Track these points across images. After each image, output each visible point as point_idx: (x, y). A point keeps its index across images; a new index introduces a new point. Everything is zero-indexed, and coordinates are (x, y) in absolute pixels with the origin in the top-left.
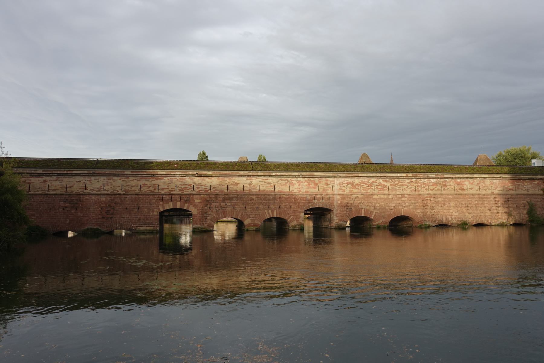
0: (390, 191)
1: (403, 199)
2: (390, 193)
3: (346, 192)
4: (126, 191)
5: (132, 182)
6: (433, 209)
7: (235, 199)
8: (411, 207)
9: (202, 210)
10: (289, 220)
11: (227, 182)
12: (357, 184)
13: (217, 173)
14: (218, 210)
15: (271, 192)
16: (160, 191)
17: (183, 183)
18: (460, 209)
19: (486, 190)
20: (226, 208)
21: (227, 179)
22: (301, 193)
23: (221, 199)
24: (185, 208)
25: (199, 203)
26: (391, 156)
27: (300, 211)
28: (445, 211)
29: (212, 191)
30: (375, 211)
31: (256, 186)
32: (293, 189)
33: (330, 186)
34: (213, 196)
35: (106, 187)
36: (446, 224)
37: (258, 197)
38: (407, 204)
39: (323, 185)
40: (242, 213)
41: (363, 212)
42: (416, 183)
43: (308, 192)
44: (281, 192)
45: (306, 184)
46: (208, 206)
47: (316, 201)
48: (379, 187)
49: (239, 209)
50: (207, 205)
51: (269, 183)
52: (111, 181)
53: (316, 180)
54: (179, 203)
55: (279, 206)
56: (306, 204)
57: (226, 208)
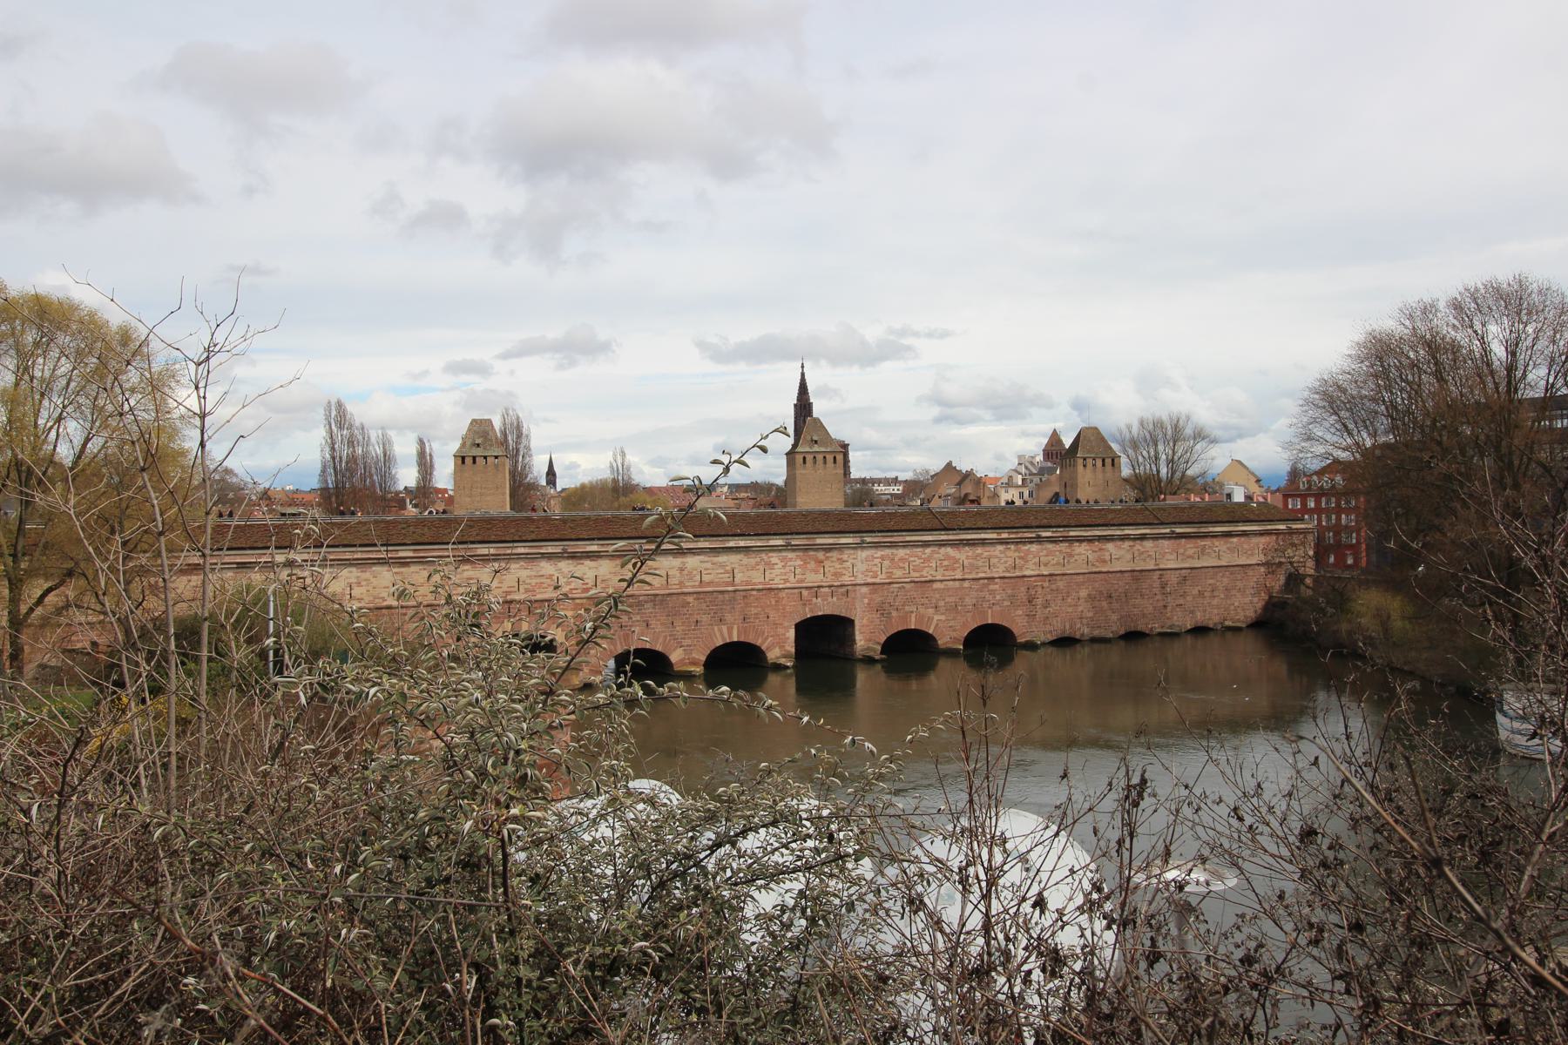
0: (966, 570)
1: (991, 587)
2: (966, 577)
3: (880, 577)
6: (1046, 605)
8: (1007, 603)
10: (763, 648)
12: (902, 559)
15: (727, 584)
17: (534, 573)
18: (1097, 603)
19: (1144, 560)
20: (631, 626)
22: (788, 585)
26: (803, 367)
27: (786, 624)
28: (1070, 610)
30: (936, 618)
31: (695, 572)
32: (772, 576)
36: (1072, 636)
38: (998, 597)
40: (666, 637)
41: (913, 619)
42: (1015, 551)
43: (802, 581)
44: (748, 583)
47: (819, 599)
48: (946, 563)
51: (722, 566)
52: (367, 575)
53: (820, 555)
55: (742, 617)
57: (631, 626)
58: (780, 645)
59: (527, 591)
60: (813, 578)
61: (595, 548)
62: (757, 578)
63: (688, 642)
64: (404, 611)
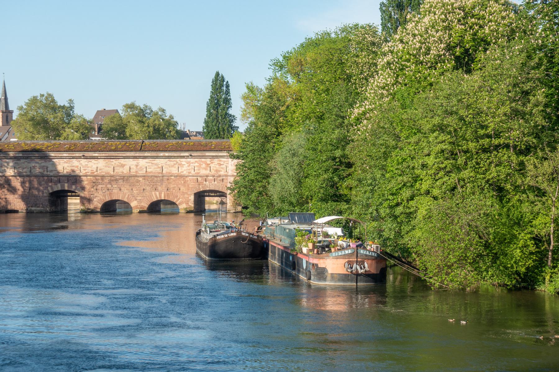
5: (23, 164)
11: (113, 163)
14: (104, 191)
15: (159, 173)
16: (48, 173)
17: (70, 165)
21: (113, 160)
22: (191, 174)
23: (106, 181)
27: (189, 193)
29: (98, 172)
31: (143, 167)
32: (183, 170)
37: (145, 179)
39: (215, 166)
40: (129, 195)
43: (198, 173)
44: (169, 173)
45: (196, 164)
46: (95, 188)
47: (207, 182)
49: (126, 191)
50: (94, 186)
51: (156, 164)
53: (208, 161)
60: (203, 172)
61: (96, 155)
62: (174, 171)
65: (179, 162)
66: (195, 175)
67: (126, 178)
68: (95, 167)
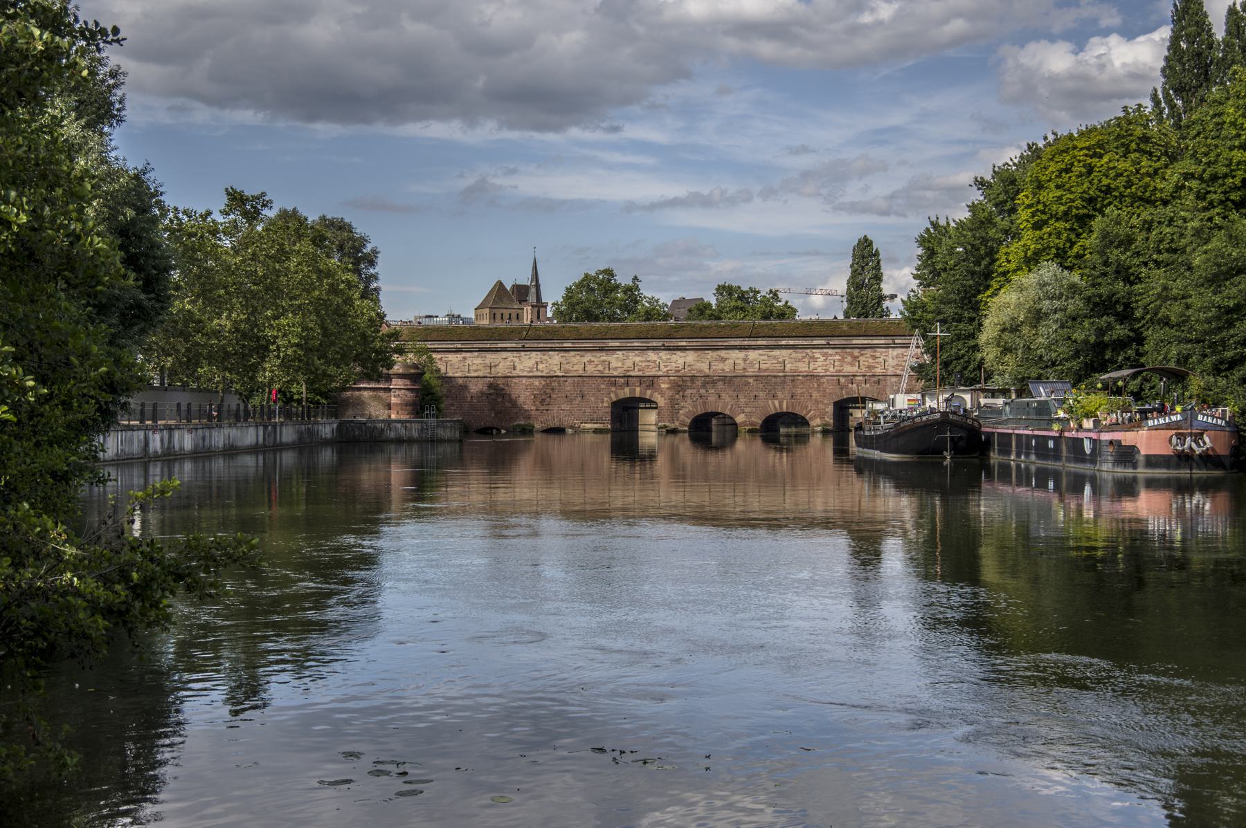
4: (567, 371)
5: (573, 359)
7: (721, 383)
9: (672, 399)
10: (807, 418)
13: (695, 343)
15: (779, 371)
21: (709, 352)
22: (828, 373)
23: (699, 383)
24: (647, 397)
25: (667, 389)
27: (826, 402)
33: (881, 360)
34: (688, 379)
35: (540, 367)
37: (757, 380)
40: (732, 405)
43: (840, 371)
44: (795, 371)
46: (681, 394)
47: (855, 385)
51: (775, 358)
52: (546, 357)
53: (856, 352)
54: (638, 389)
56: (838, 391)
58: (820, 416)
59: (639, 370)
60: (848, 369)
61: (684, 344)
62: (803, 367)
63: (750, 410)
64: (565, 379)
65: (810, 353)
66: (835, 374)
67: (727, 380)
68: (681, 361)
